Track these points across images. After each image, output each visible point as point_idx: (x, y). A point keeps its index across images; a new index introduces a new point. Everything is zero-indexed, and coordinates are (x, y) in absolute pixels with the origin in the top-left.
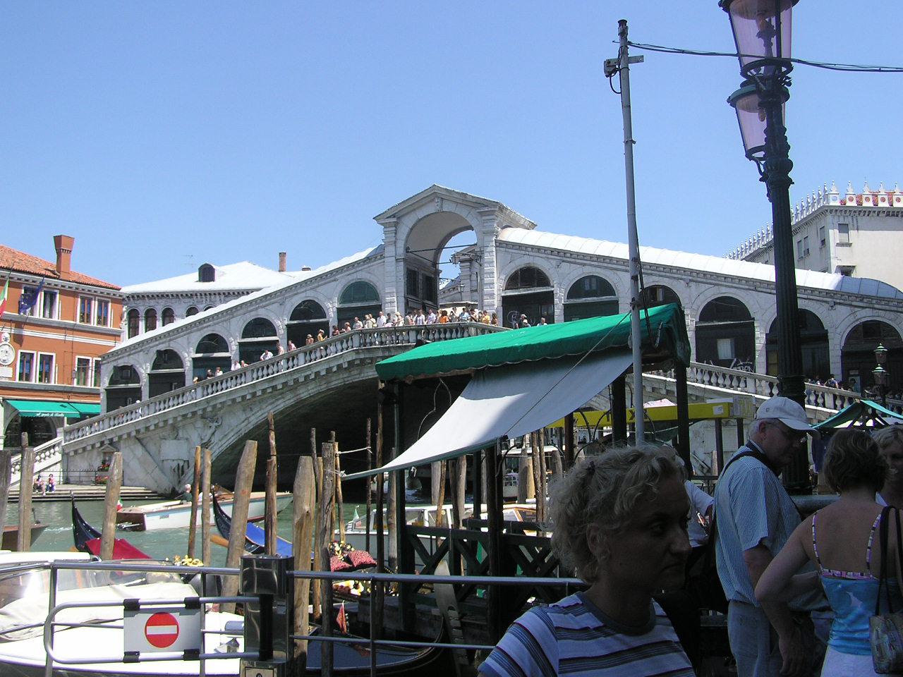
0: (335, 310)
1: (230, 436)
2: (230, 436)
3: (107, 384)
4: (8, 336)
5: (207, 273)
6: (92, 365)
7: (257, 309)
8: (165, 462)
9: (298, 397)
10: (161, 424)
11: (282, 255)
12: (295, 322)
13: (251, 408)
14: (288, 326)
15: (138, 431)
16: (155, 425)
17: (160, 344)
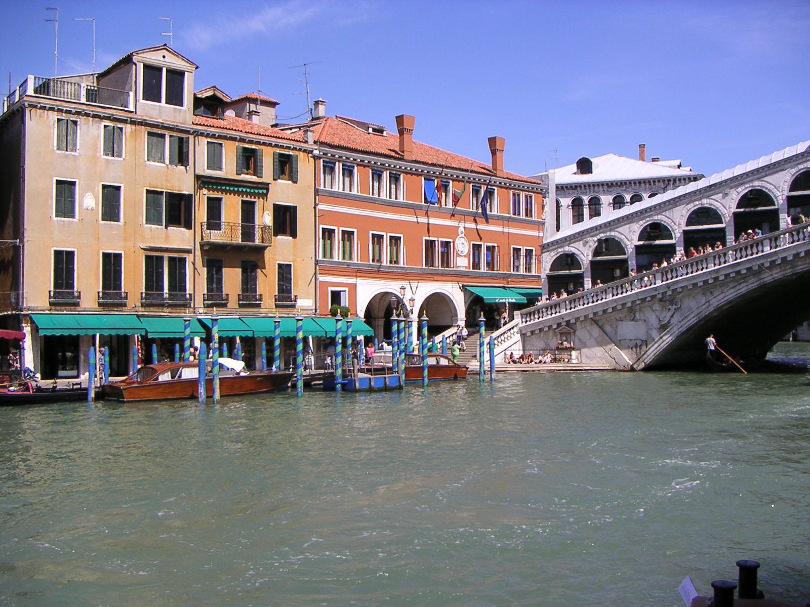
0: (784, 197)
1: (689, 318)
2: (689, 318)
3: (548, 271)
4: (463, 229)
5: (585, 166)
6: (523, 253)
7: (700, 199)
8: (622, 341)
9: (762, 281)
10: (619, 307)
11: (642, 146)
12: (742, 210)
13: (712, 293)
14: (735, 214)
15: (595, 314)
16: (613, 308)
17: (600, 233)
